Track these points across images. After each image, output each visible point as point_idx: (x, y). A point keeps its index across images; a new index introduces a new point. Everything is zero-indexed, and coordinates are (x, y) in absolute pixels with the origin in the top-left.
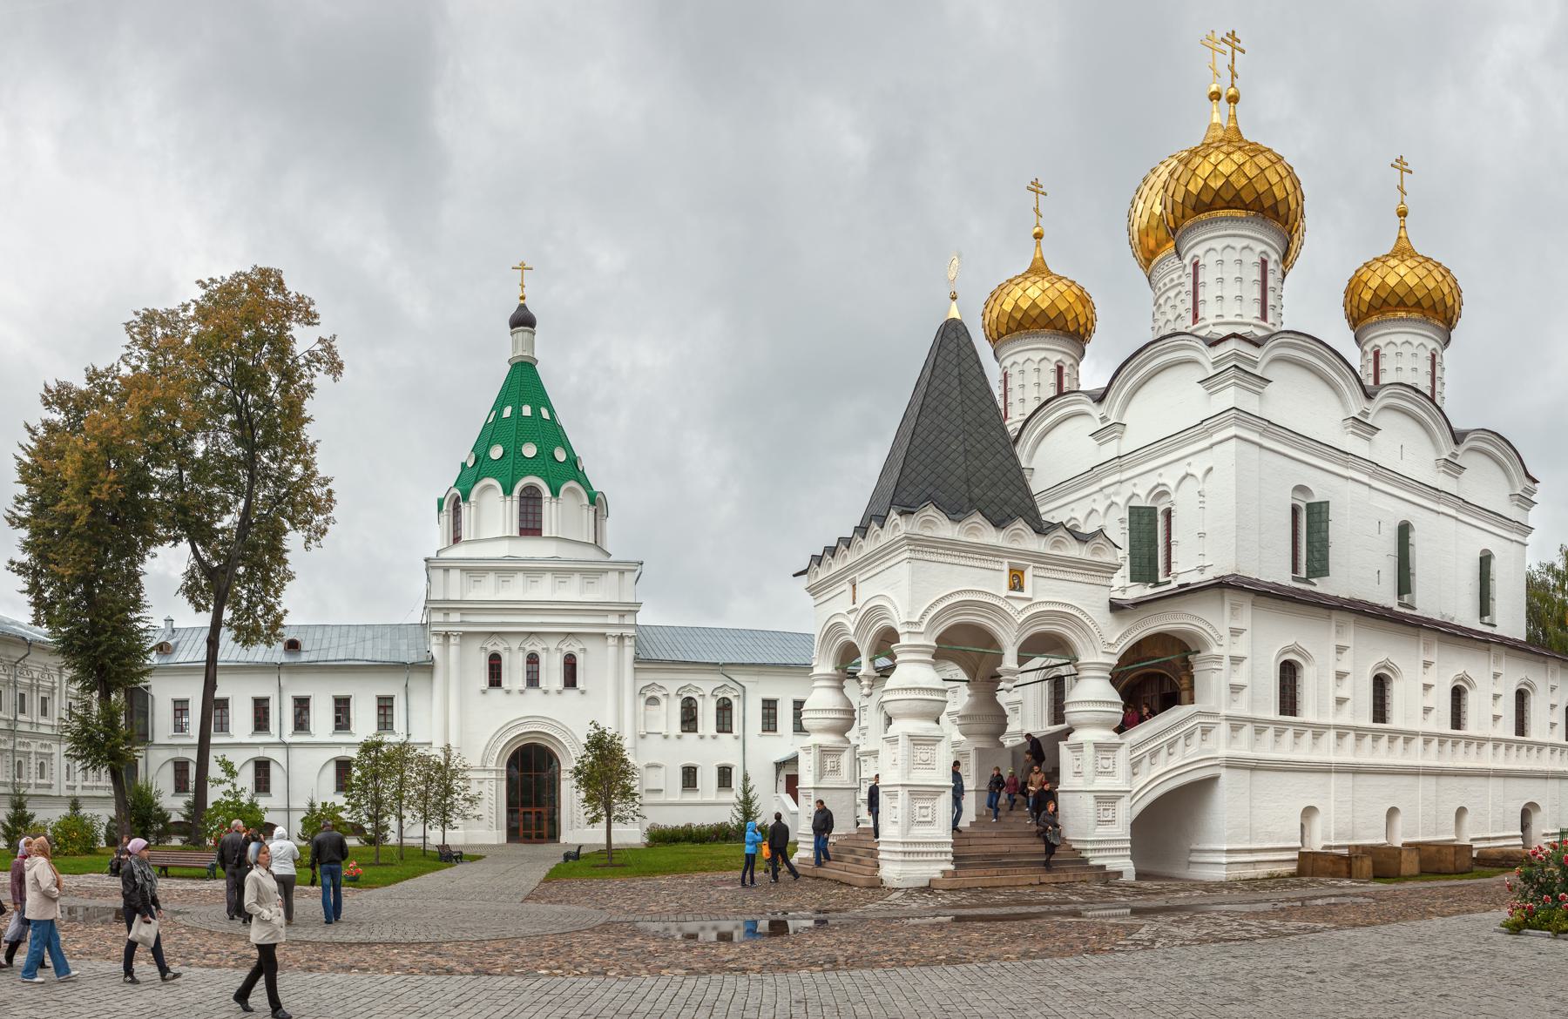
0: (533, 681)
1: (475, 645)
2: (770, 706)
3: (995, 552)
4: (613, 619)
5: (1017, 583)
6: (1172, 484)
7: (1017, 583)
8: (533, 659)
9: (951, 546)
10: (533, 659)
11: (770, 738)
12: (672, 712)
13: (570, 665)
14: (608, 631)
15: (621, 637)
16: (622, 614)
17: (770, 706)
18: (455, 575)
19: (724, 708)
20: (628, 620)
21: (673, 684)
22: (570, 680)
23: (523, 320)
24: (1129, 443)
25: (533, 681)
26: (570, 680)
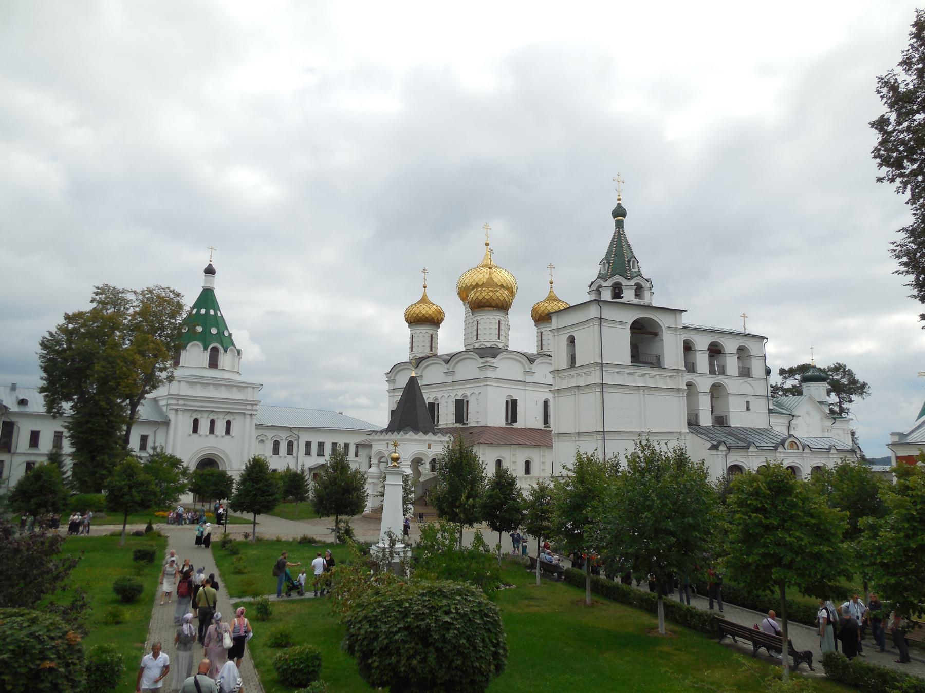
0: (212, 431)
1: (188, 414)
2: (308, 444)
3: (425, 441)
4: (249, 407)
5: (429, 448)
6: (469, 395)
7: (429, 448)
8: (213, 423)
9: (416, 440)
10: (213, 423)
11: (308, 458)
12: (269, 446)
13: (228, 423)
14: (247, 412)
15: (251, 415)
16: (252, 405)
17: (308, 444)
18: (183, 384)
19: (290, 444)
20: (255, 408)
21: (270, 434)
22: (228, 431)
23: (210, 271)
24: (458, 377)
25: (212, 431)
26: (228, 431)
